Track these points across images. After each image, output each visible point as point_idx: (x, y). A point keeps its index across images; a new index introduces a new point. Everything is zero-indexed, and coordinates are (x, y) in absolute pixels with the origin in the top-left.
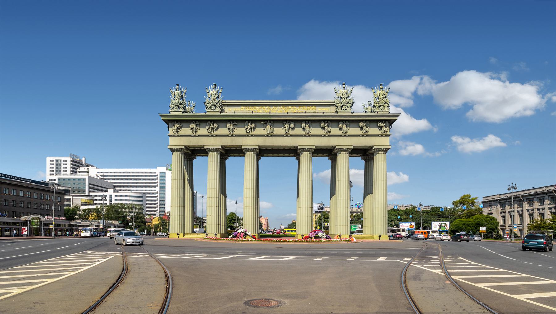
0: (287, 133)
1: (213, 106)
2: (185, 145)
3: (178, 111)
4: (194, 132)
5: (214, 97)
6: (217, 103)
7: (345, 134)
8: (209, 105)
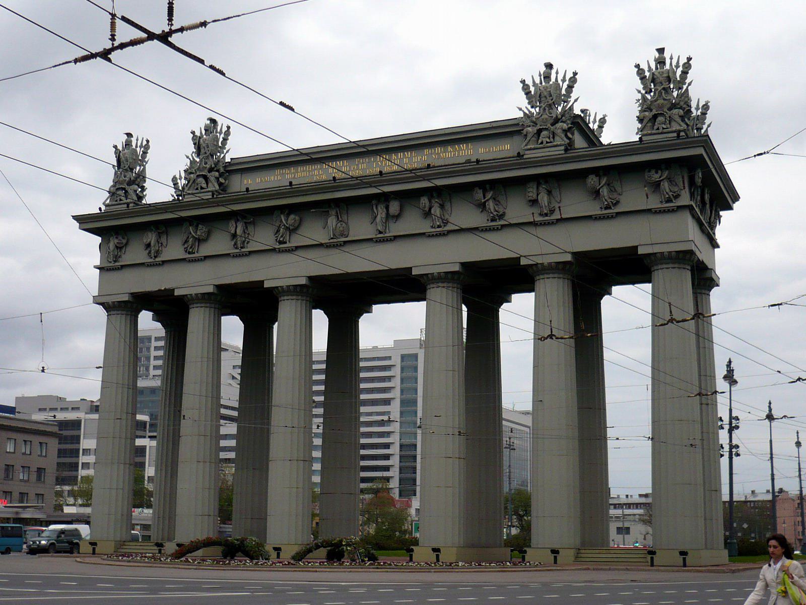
0: (380, 233)
1: (201, 180)
2: (132, 291)
3: (121, 202)
4: (153, 256)
5: (206, 153)
6: (211, 170)
7: (546, 218)
8: (192, 175)
